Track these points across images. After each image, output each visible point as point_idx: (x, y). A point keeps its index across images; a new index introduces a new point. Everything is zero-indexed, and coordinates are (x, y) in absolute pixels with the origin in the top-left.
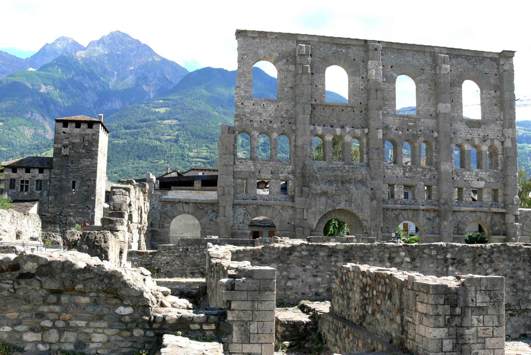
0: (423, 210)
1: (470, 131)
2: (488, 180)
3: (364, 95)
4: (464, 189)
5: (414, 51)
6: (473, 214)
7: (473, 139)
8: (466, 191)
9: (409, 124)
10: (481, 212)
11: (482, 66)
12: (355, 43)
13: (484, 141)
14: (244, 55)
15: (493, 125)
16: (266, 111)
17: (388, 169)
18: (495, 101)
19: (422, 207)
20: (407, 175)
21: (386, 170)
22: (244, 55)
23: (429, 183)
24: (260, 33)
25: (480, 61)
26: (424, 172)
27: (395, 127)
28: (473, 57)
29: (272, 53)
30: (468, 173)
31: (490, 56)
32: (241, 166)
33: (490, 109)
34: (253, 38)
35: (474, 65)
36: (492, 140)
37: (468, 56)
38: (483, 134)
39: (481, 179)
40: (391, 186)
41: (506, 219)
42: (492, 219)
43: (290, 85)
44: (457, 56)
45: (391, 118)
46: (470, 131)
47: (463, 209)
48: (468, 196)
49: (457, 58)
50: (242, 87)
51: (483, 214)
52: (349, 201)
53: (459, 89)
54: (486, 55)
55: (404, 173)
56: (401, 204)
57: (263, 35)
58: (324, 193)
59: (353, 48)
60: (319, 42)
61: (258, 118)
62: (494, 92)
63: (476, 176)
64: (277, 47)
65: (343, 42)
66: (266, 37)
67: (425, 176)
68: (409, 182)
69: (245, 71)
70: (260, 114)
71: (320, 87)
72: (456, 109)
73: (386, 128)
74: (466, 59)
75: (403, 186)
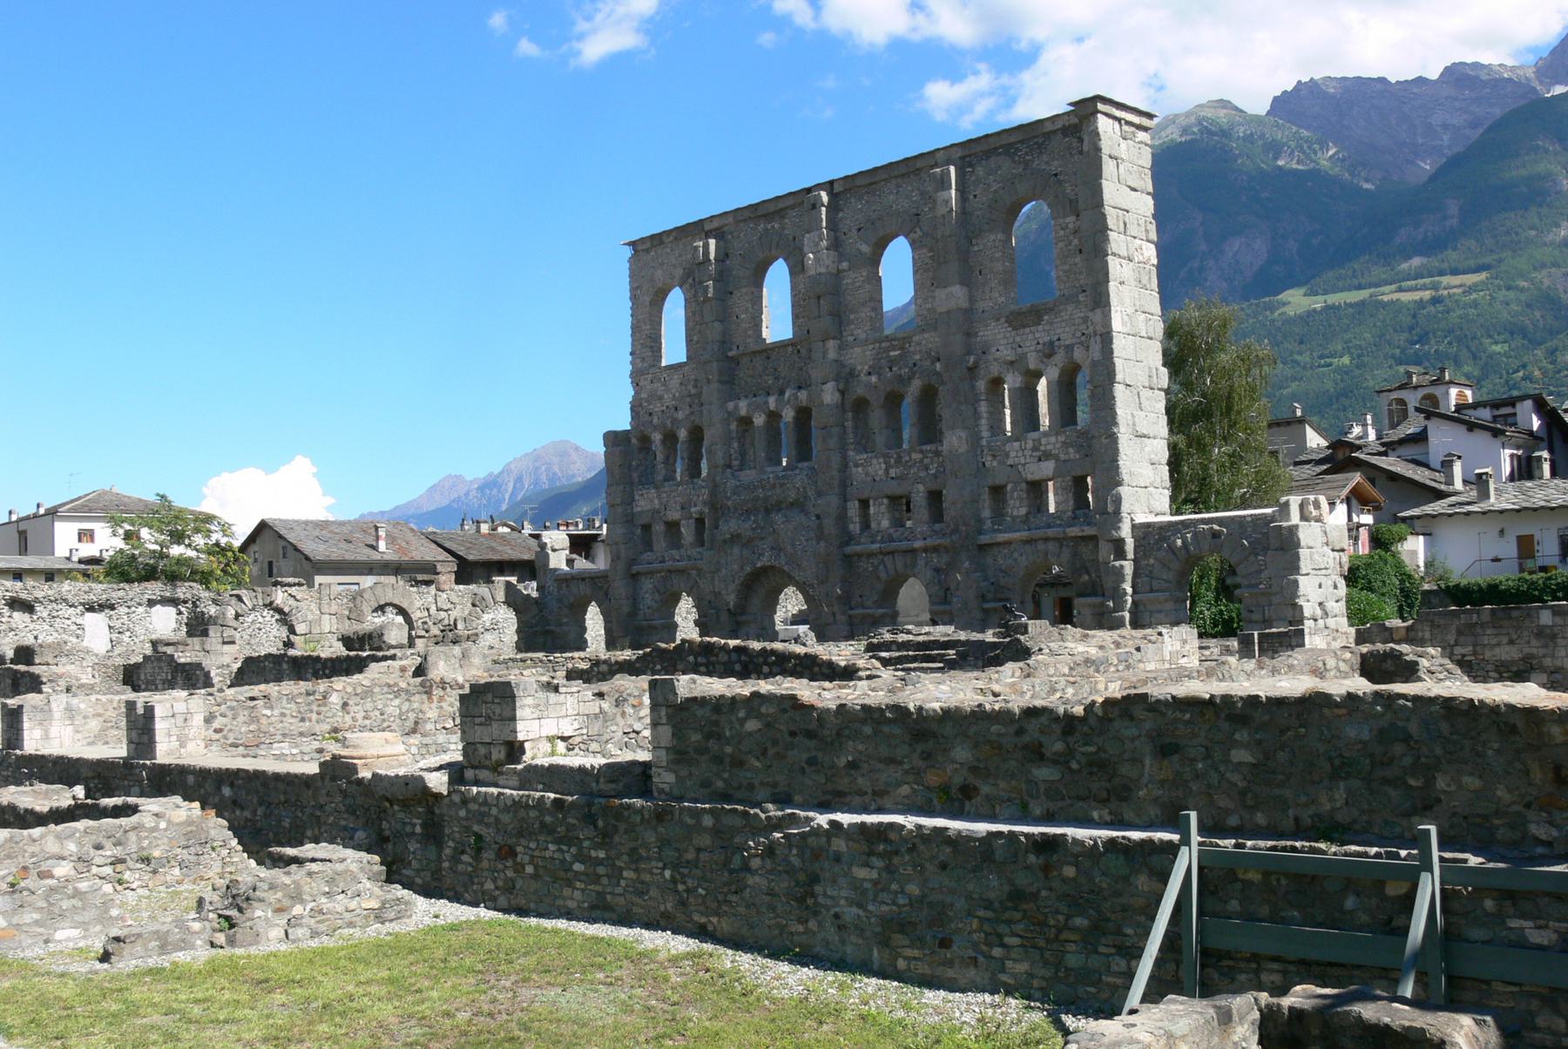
0: (925, 550)
1: (1018, 339)
2: (1062, 457)
4: (1009, 487)
5: (896, 177)
6: (1028, 547)
7: (1023, 356)
8: (1013, 490)
10: (1046, 539)
11: (1045, 158)
12: (790, 202)
13: (1050, 356)
15: (1070, 308)
16: (668, 390)
17: (857, 466)
18: (1076, 242)
19: (918, 544)
20: (893, 472)
23: (934, 486)
24: (652, 237)
25: (1040, 146)
26: (926, 461)
28: (1022, 142)
30: (1016, 444)
31: (1059, 125)
32: (642, 503)
33: (1066, 267)
34: (647, 251)
35: (1027, 164)
36: (1070, 348)
37: (1010, 145)
38: (1047, 339)
39: (1047, 456)
40: (865, 504)
42: (1075, 554)
44: (988, 154)
45: (858, 350)
46: (1018, 339)
47: (1002, 537)
49: (988, 158)
51: (1051, 546)
52: (777, 549)
53: (992, 237)
54: (1049, 127)
55: (887, 470)
56: (882, 541)
57: (657, 239)
58: (735, 538)
59: (792, 213)
60: (737, 222)
61: (657, 407)
62: (1073, 218)
63: (1035, 449)
65: (771, 208)
66: (662, 243)
67: (927, 469)
68: (896, 489)
70: (661, 398)
72: (987, 290)
73: (845, 377)
74: (1007, 154)
75: (885, 501)
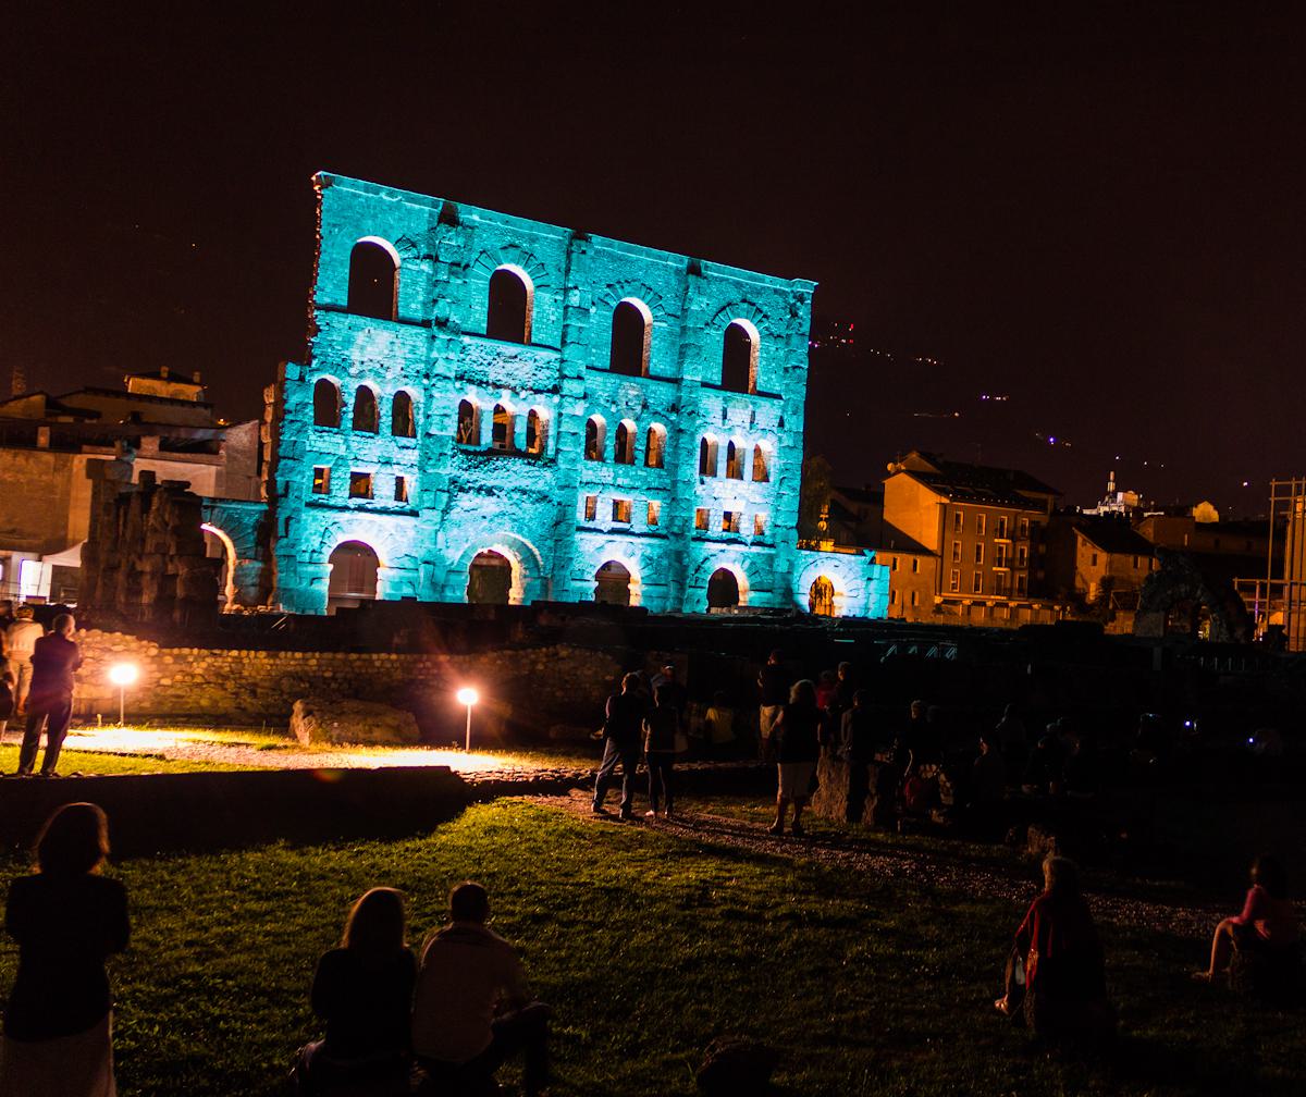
3: (556, 333)
9: (630, 392)
14: (334, 225)
20: (620, 481)
21: (584, 471)
22: (334, 225)
27: (606, 394)
29: (390, 231)
32: (319, 444)
33: (766, 379)
41: (774, 566)
43: (421, 298)
48: (717, 523)
50: (327, 290)
55: (615, 478)
64: (401, 219)
69: (334, 260)
71: (477, 307)
